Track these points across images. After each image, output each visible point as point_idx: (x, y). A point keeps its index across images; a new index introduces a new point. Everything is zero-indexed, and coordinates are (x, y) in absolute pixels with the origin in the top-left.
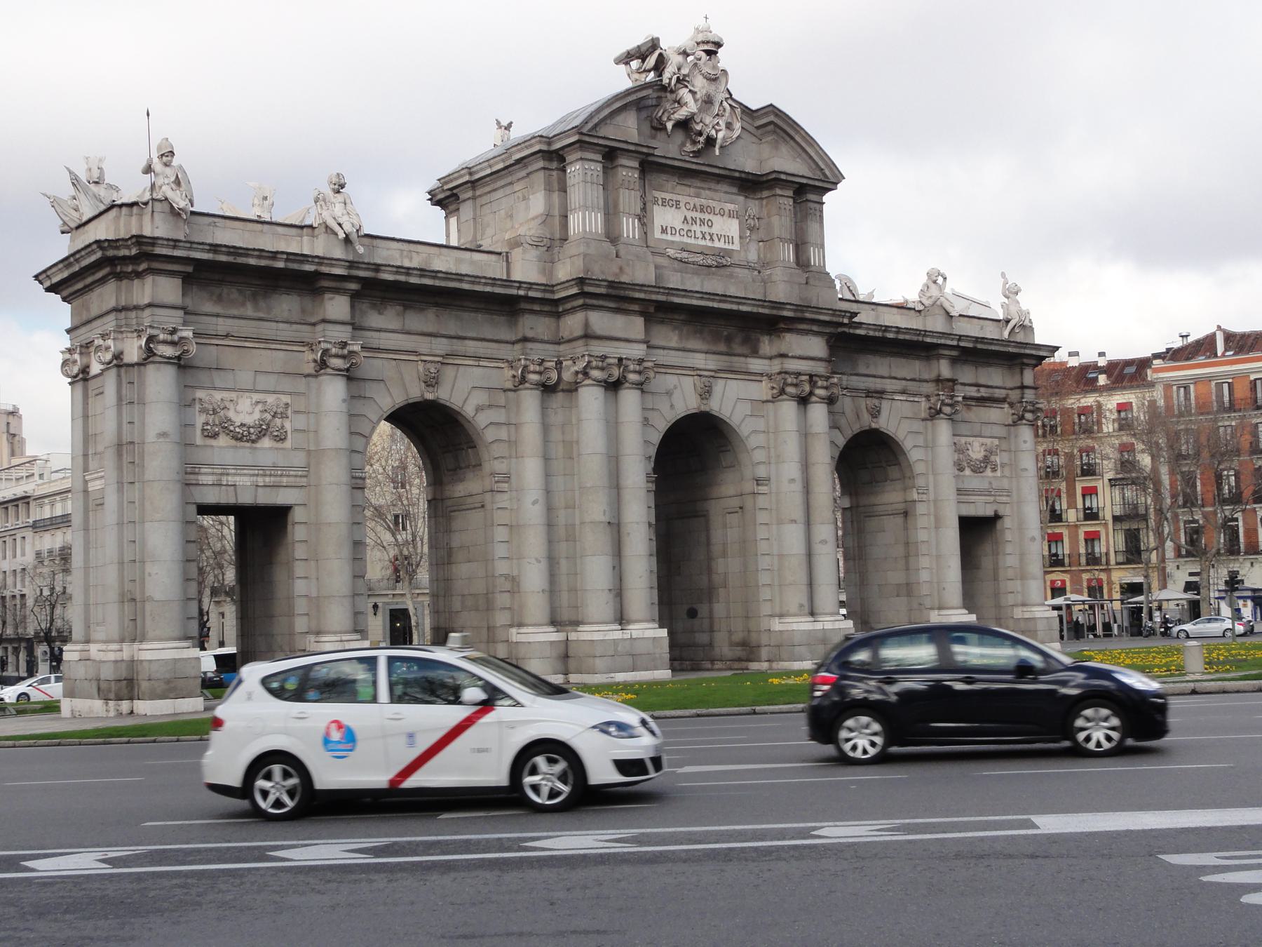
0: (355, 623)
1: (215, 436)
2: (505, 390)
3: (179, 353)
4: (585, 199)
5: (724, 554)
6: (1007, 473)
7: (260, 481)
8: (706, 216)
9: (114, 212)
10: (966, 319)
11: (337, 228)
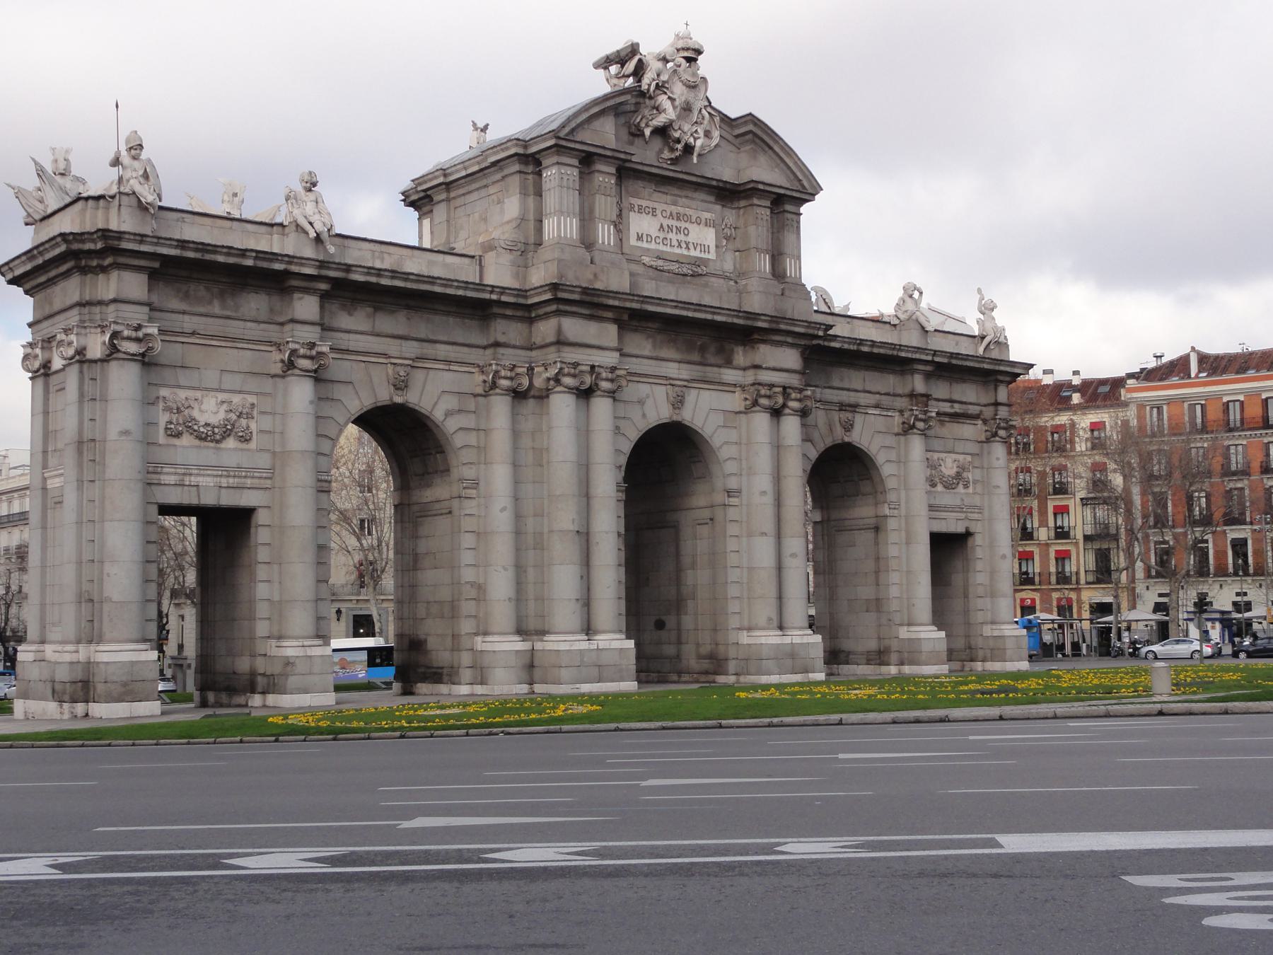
0: (318, 629)
1: (178, 435)
2: (476, 396)
3: (144, 350)
4: (561, 204)
5: (693, 566)
6: (979, 489)
7: (224, 482)
8: (683, 225)
9: (80, 205)
10: (941, 334)
11: (308, 227)
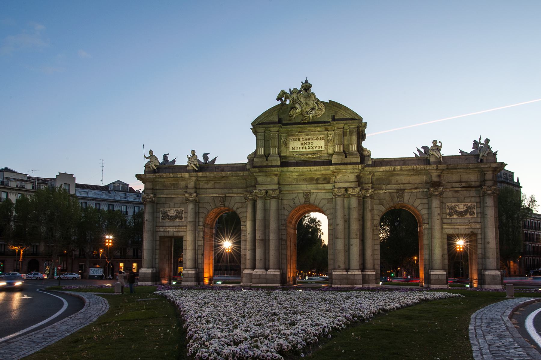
1: (164, 219)
8: (311, 141)
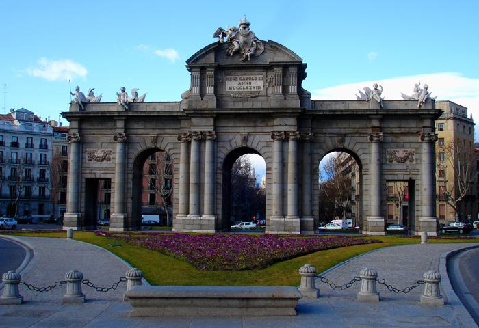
1: (91, 160)
7: (102, 172)
